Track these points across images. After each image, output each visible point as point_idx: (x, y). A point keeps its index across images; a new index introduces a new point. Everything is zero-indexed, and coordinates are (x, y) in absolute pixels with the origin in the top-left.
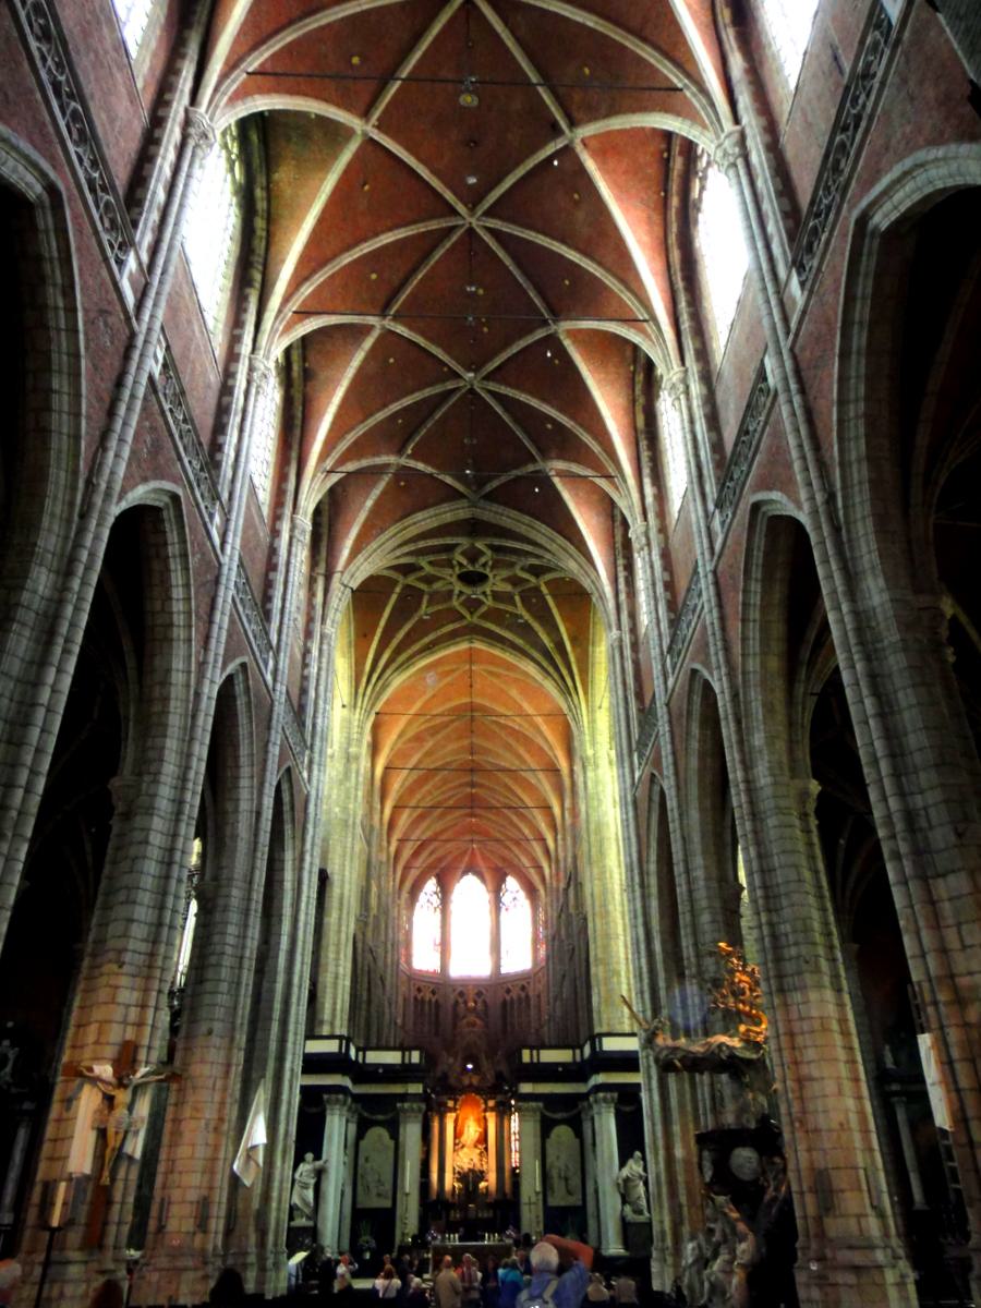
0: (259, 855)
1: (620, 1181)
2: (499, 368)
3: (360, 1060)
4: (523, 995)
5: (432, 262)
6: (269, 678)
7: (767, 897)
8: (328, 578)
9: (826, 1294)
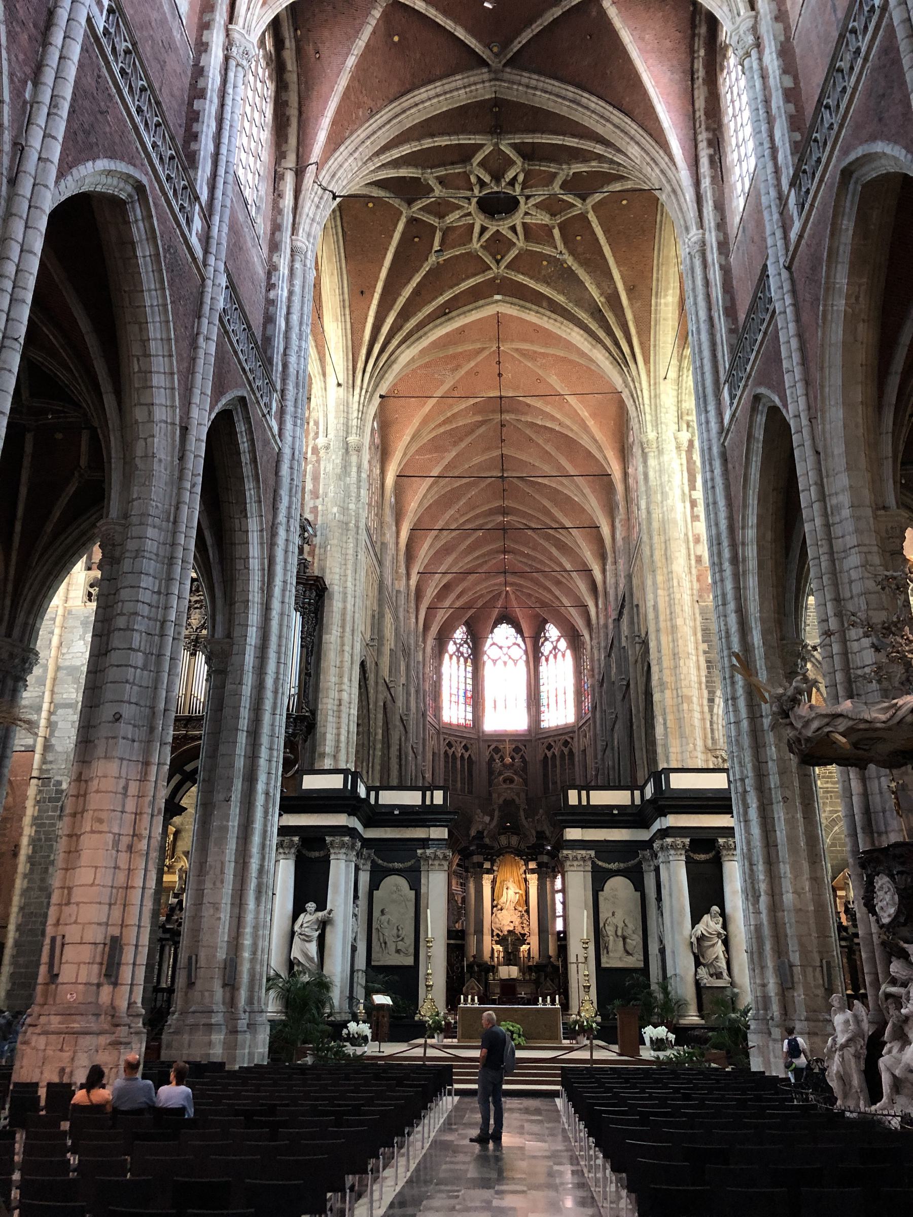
1: (694, 940)
3: (372, 801)
4: (566, 751)
8: (299, 173)
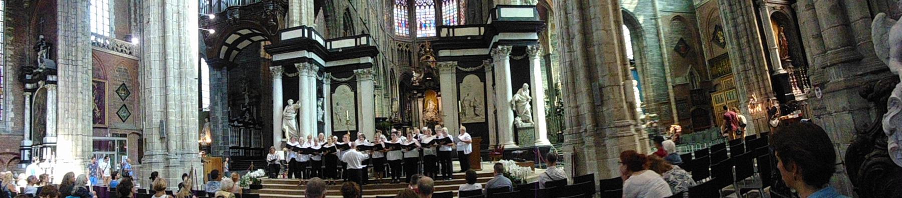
1: (514, 103)
3: (328, 48)
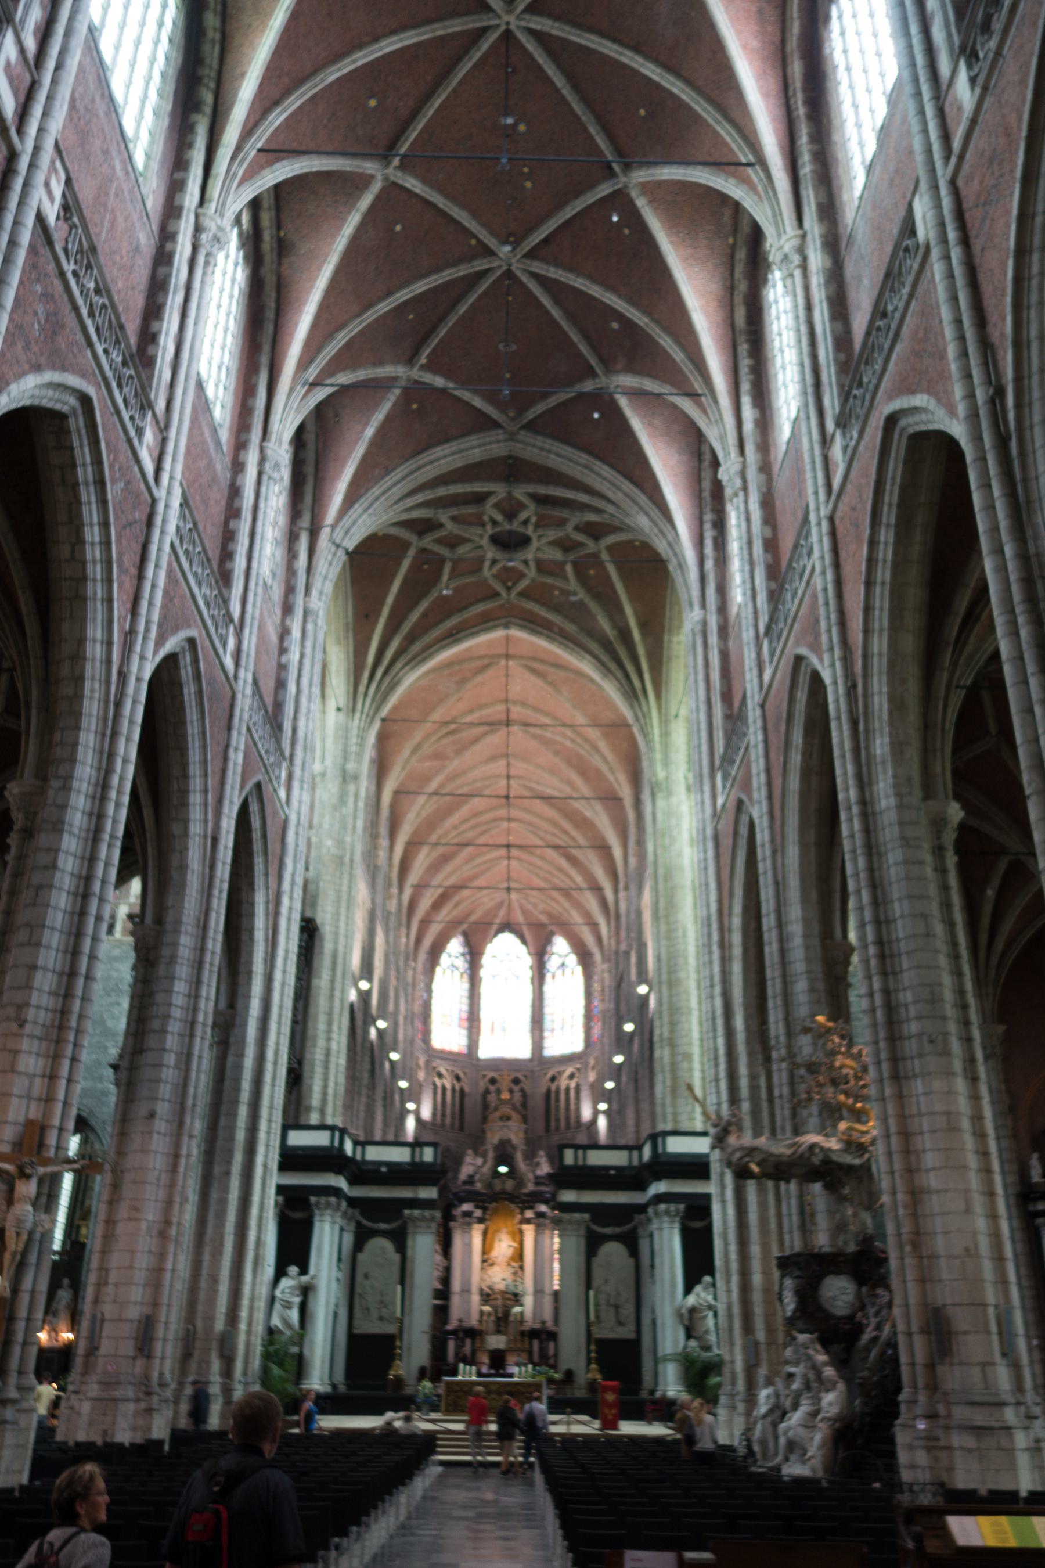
0: (216, 892)
1: (684, 1311)
2: (546, 241)
5: (455, 82)
6: (229, 662)
7: (882, 957)
9: (936, 1459)
